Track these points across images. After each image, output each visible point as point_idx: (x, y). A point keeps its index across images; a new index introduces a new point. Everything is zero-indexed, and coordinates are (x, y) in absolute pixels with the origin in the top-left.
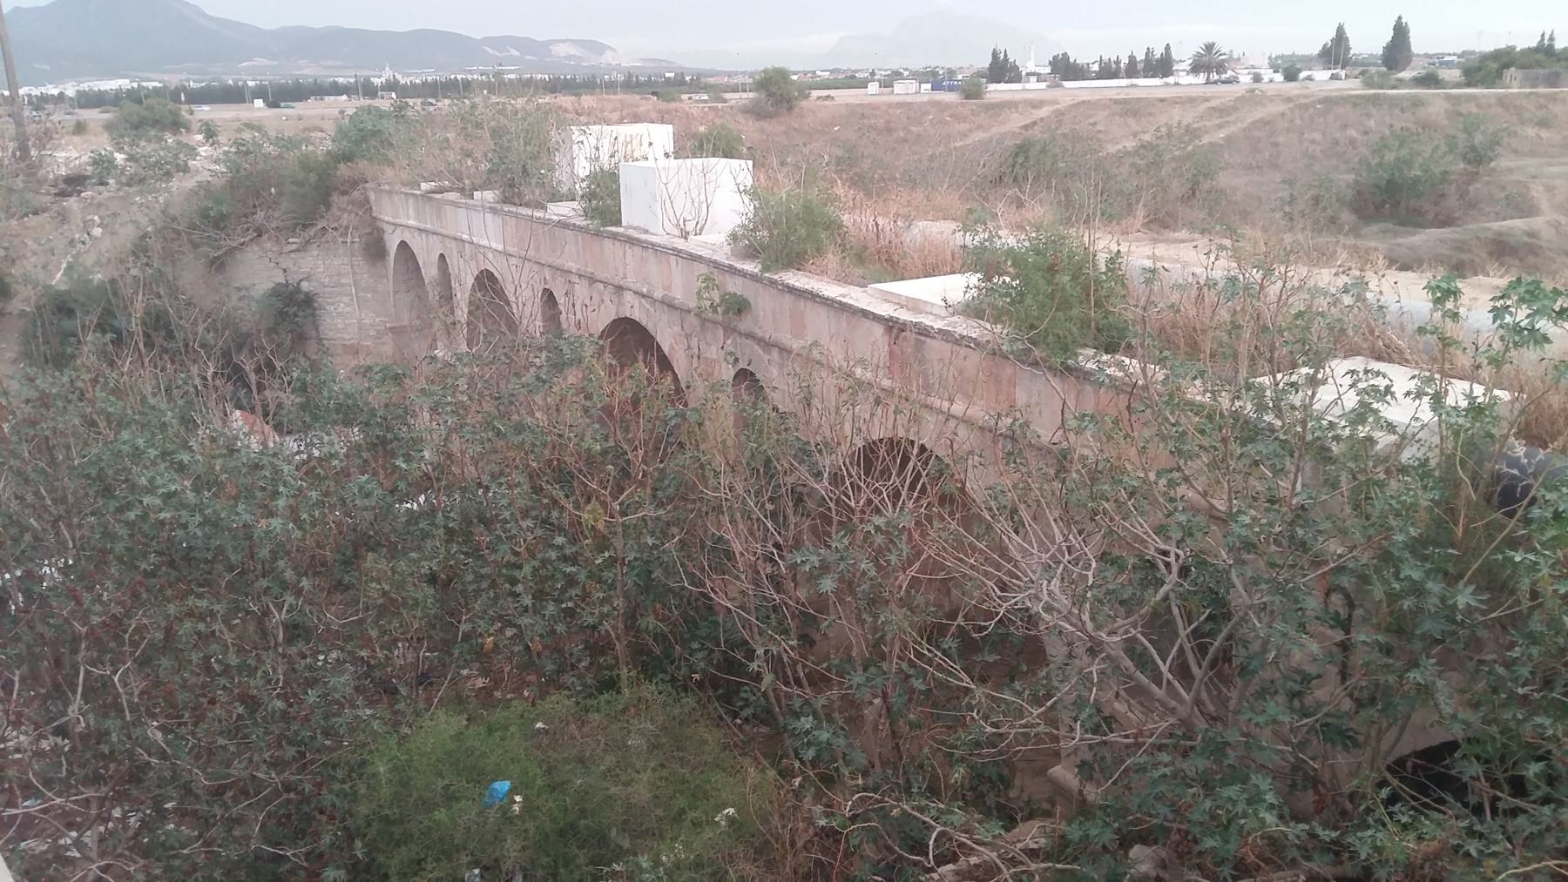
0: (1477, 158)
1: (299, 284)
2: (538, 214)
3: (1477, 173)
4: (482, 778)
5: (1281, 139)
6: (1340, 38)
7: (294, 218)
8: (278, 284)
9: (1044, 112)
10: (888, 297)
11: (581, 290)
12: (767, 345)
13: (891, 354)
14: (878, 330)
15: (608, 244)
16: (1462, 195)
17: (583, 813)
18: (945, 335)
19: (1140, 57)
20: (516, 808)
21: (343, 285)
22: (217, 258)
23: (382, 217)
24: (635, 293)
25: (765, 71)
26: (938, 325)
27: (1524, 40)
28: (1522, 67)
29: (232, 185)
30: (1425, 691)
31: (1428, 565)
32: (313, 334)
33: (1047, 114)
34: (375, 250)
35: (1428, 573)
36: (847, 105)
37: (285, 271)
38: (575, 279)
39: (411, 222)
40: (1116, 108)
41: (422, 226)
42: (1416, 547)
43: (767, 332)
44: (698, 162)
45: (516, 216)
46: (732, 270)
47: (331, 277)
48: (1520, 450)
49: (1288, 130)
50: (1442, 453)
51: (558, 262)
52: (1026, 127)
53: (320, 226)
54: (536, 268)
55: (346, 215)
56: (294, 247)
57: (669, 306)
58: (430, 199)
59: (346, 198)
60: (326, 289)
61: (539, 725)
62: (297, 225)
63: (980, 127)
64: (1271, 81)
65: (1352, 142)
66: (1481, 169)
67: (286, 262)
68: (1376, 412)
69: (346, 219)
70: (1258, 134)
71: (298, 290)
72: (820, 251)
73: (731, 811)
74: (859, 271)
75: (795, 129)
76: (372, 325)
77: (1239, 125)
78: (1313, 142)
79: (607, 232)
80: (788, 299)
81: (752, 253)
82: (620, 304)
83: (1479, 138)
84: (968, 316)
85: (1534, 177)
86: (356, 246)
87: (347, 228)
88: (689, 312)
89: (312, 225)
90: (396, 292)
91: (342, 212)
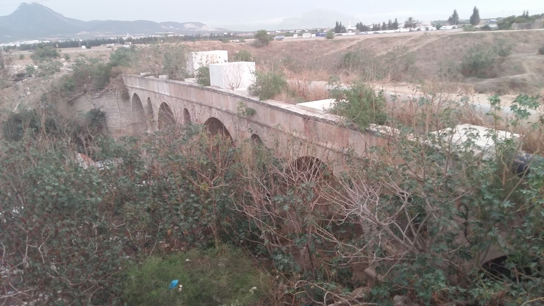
0: (504, 54)
2: (182, 82)
3: (504, 59)
4: (168, 279)
5: (436, 50)
6: (455, 15)
7: (97, 86)
9: (355, 43)
10: (303, 108)
11: (197, 108)
12: (262, 125)
13: (305, 127)
14: (301, 119)
15: (206, 92)
17: (204, 290)
18: (324, 120)
19: (387, 23)
20: (180, 289)
21: (115, 109)
22: (71, 101)
23: (127, 85)
24: (216, 109)
25: (258, 31)
26: (321, 117)
27: (518, 13)
28: (518, 22)
30: (494, 239)
31: (494, 195)
32: (105, 126)
34: (126, 97)
35: (494, 197)
36: (287, 42)
37: (94, 105)
38: (195, 105)
39: (138, 87)
41: (141, 88)
42: (490, 189)
43: (262, 121)
44: (236, 63)
45: (174, 83)
46: (250, 100)
47: (110, 106)
48: (524, 154)
49: (439, 47)
50: (497, 156)
51: (189, 99)
52: (348, 48)
54: (181, 101)
55: (115, 85)
56: (97, 96)
58: (144, 78)
61: (187, 260)
63: (333, 49)
64: (432, 30)
65: (461, 50)
66: (505, 58)
67: (95, 102)
68: (474, 142)
69: (115, 86)
71: (99, 111)
72: (279, 93)
73: (255, 288)
74: (293, 99)
75: (270, 51)
77: (422, 45)
78: (447, 50)
79: (206, 88)
80: (269, 109)
81: (256, 94)
82: (211, 113)
83: (504, 47)
84: (332, 114)
85: (524, 60)
86: (119, 95)
87: (115, 89)
88: (235, 115)
89: (103, 89)
90: (133, 111)
91: (113, 84)
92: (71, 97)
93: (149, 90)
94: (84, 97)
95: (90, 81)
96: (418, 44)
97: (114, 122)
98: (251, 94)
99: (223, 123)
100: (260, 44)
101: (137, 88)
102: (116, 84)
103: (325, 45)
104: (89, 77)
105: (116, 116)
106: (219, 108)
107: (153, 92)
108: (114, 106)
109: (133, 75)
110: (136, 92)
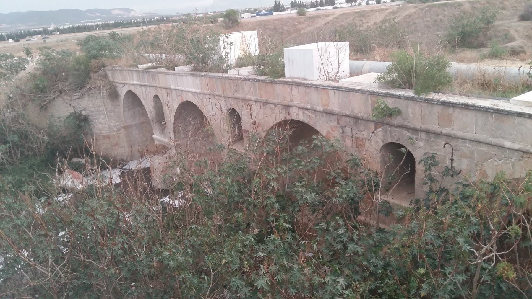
1: (81, 112)
3: (488, 28)
5: (416, 21)
7: (76, 85)
8: (72, 113)
9: (331, 18)
11: (256, 108)
12: (415, 130)
15: (279, 88)
16: (485, 36)
21: (100, 111)
22: (44, 105)
23: (116, 81)
24: (299, 108)
25: (227, 11)
29: (45, 73)
32: (90, 133)
33: (332, 19)
34: (114, 95)
37: (74, 107)
38: (254, 103)
39: (135, 82)
40: (357, 15)
41: (142, 83)
45: (213, 77)
46: (387, 95)
47: (95, 108)
52: (325, 24)
53: (88, 87)
55: (98, 82)
56: (77, 97)
57: (327, 113)
58: (147, 72)
59: (96, 74)
60: (94, 113)
62: (77, 88)
64: (372, 4)
67: (75, 104)
69: (99, 83)
70: (408, 20)
71: (80, 115)
76: (115, 126)
77: (401, 17)
78: (428, 21)
79: (280, 81)
80: (437, 109)
85: (510, 27)
86: (105, 94)
87: (100, 87)
90: (124, 111)
91: (96, 80)
92: (45, 101)
93: (157, 85)
94: (60, 99)
95: (66, 79)
96: (397, 17)
97: (100, 126)
98: (379, 87)
99: (314, 126)
100: (230, 25)
101: (133, 84)
102: (100, 80)
103: (300, 23)
104: (63, 74)
105: (103, 119)
106: (309, 107)
107: (165, 88)
108: (99, 107)
109: (126, 68)
110: (132, 89)
